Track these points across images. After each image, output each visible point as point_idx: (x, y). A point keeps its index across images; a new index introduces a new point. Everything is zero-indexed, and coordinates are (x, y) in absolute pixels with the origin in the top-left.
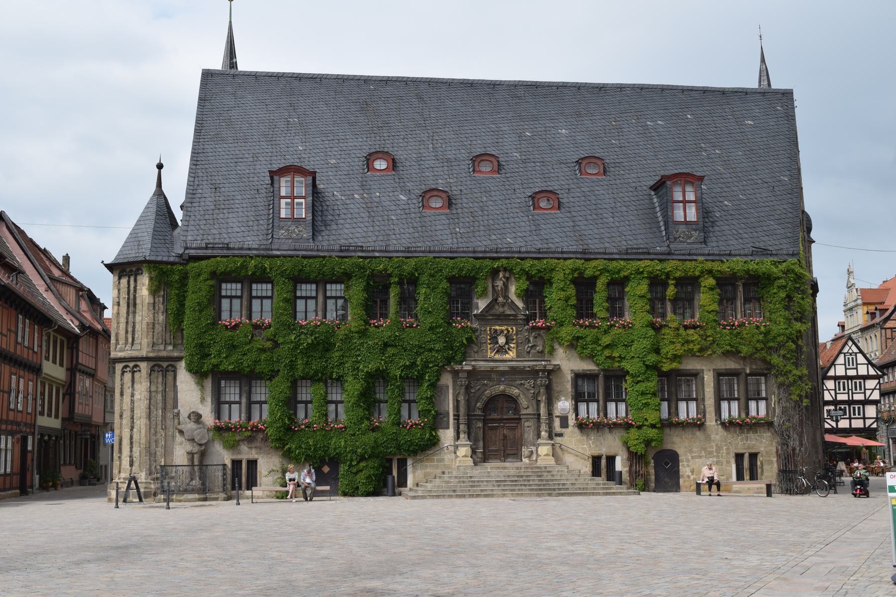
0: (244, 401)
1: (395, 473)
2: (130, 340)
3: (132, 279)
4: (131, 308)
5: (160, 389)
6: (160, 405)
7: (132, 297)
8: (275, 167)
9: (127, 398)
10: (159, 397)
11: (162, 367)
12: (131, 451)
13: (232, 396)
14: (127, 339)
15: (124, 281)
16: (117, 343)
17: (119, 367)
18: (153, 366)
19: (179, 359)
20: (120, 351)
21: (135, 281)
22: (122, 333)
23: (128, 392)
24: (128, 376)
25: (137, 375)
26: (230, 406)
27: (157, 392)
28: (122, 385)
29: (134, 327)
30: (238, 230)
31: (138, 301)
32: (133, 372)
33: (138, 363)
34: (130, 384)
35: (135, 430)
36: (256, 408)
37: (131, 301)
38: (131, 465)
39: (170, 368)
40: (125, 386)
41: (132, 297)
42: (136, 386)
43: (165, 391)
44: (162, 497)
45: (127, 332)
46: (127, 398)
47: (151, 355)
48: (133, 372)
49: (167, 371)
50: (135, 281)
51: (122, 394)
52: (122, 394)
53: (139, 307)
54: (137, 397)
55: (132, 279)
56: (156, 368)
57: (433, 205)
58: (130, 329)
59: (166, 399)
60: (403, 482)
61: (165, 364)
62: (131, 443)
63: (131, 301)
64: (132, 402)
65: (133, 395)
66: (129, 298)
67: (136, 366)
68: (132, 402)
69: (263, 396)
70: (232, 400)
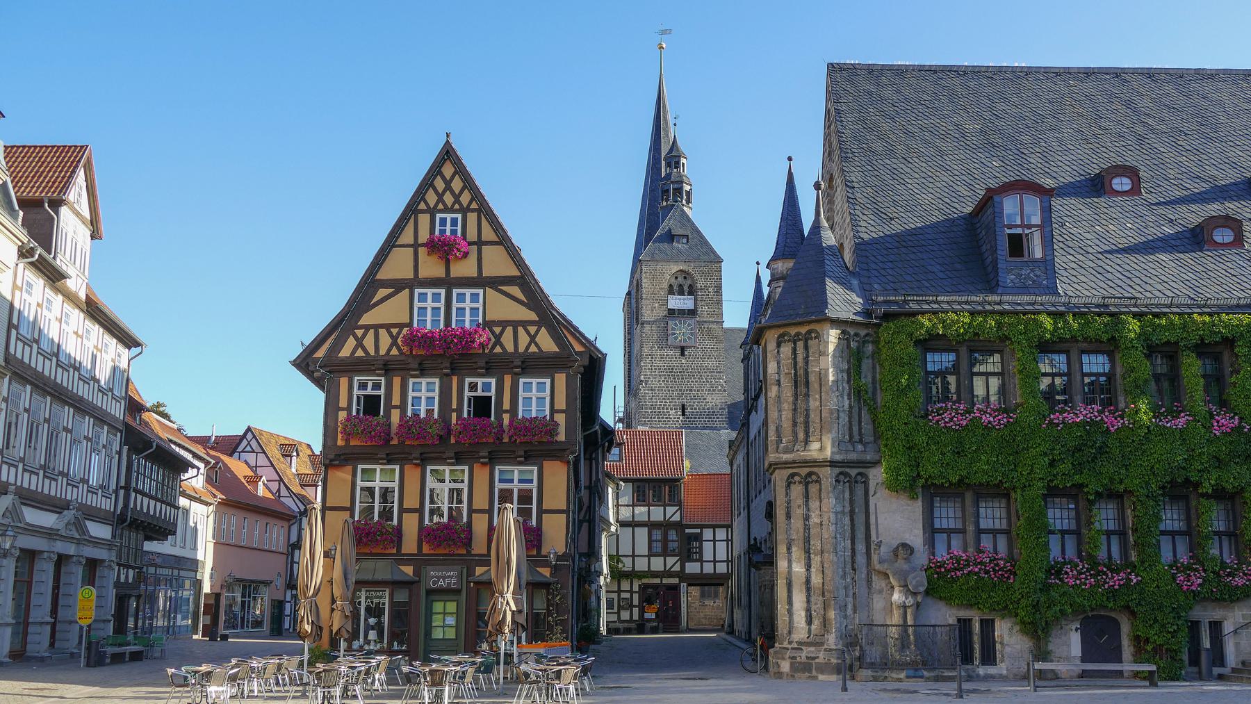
0: (971, 528)
1: (1206, 643)
2: (801, 436)
3: (800, 344)
4: (802, 389)
5: (847, 509)
6: (848, 533)
7: (801, 372)
8: (993, 184)
9: (797, 523)
10: (847, 520)
11: (850, 474)
12: (808, 601)
13: (944, 521)
14: (795, 434)
15: (786, 349)
16: (779, 441)
17: (780, 476)
18: (841, 473)
19: (876, 463)
20: (785, 453)
21: (806, 348)
22: (787, 425)
23: (798, 512)
24: (797, 490)
25: (813, 489)
26: (949, 537)
27: (843, 513)
28: (788, 502)
29: (807, 416)
30: (941, 275)
31: (812, 378)
32: (807, 484)
33: (815, 469)
34: (800, 501)
35: (813, 570)
36: (941, 540)
37: (801, 379)
38: (809, 621)
39: (859, 478)
40: (794, 505)
41: (801, 372)
42: (814, 504)
43: (852, 512)
44: (870, 672)
45: (795, 424)
46: (797, 523)
47: (838, 458)
48: (807, 484)
49: (856, 482)
50: (806, 348)
51: (788, 516)
52: (788, 516)
53: (814, 385)
54: (814, 519)
55: (800, 344)
56: (841, 478)
57: (1218, 239)
58: (800, 420)
59: (858, 520)
60: (1218, 656)
61: (853, 472)
62: (808, 590)
63: (801, 379)
64: (807, 528)
65: (807, 518)
66: (796, 374)
67: (810, 474)
68: (807, 528)
69: (997, 521)
70: (952, 526)
